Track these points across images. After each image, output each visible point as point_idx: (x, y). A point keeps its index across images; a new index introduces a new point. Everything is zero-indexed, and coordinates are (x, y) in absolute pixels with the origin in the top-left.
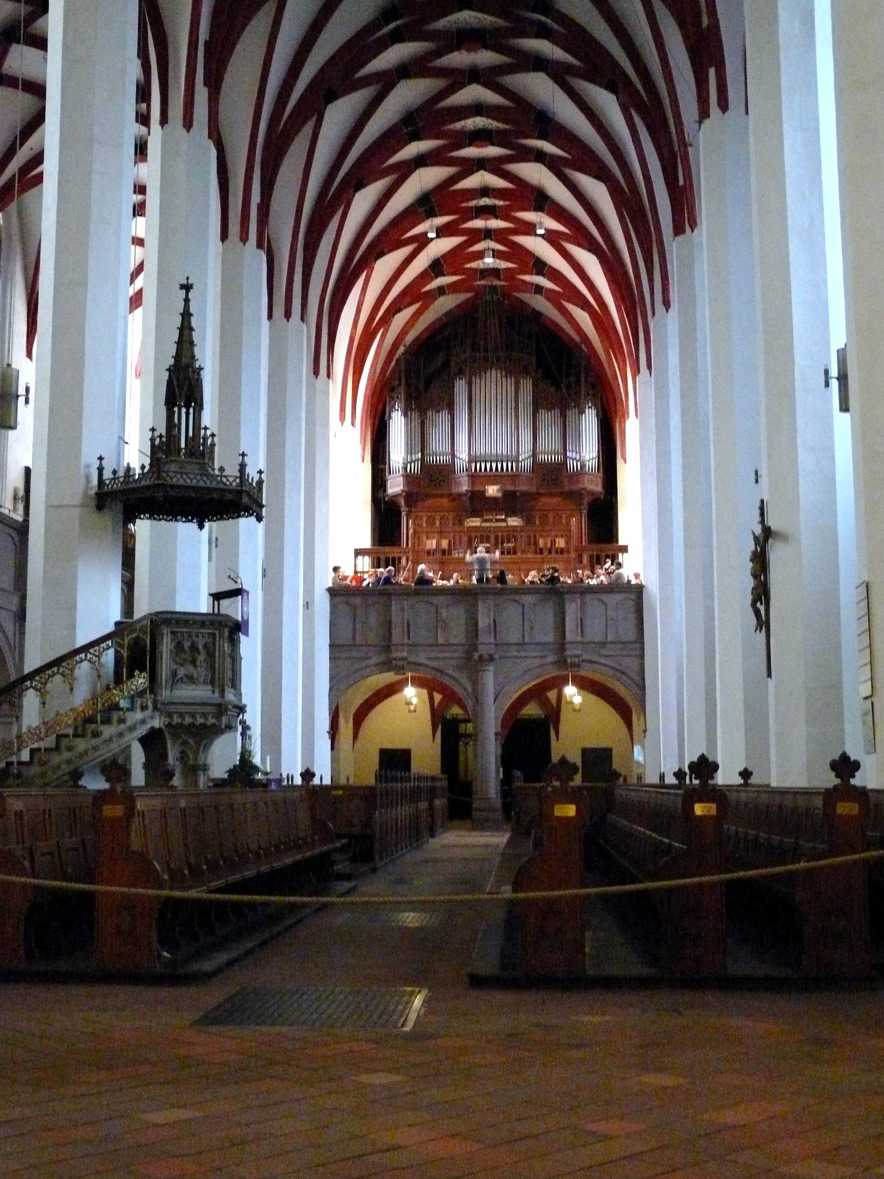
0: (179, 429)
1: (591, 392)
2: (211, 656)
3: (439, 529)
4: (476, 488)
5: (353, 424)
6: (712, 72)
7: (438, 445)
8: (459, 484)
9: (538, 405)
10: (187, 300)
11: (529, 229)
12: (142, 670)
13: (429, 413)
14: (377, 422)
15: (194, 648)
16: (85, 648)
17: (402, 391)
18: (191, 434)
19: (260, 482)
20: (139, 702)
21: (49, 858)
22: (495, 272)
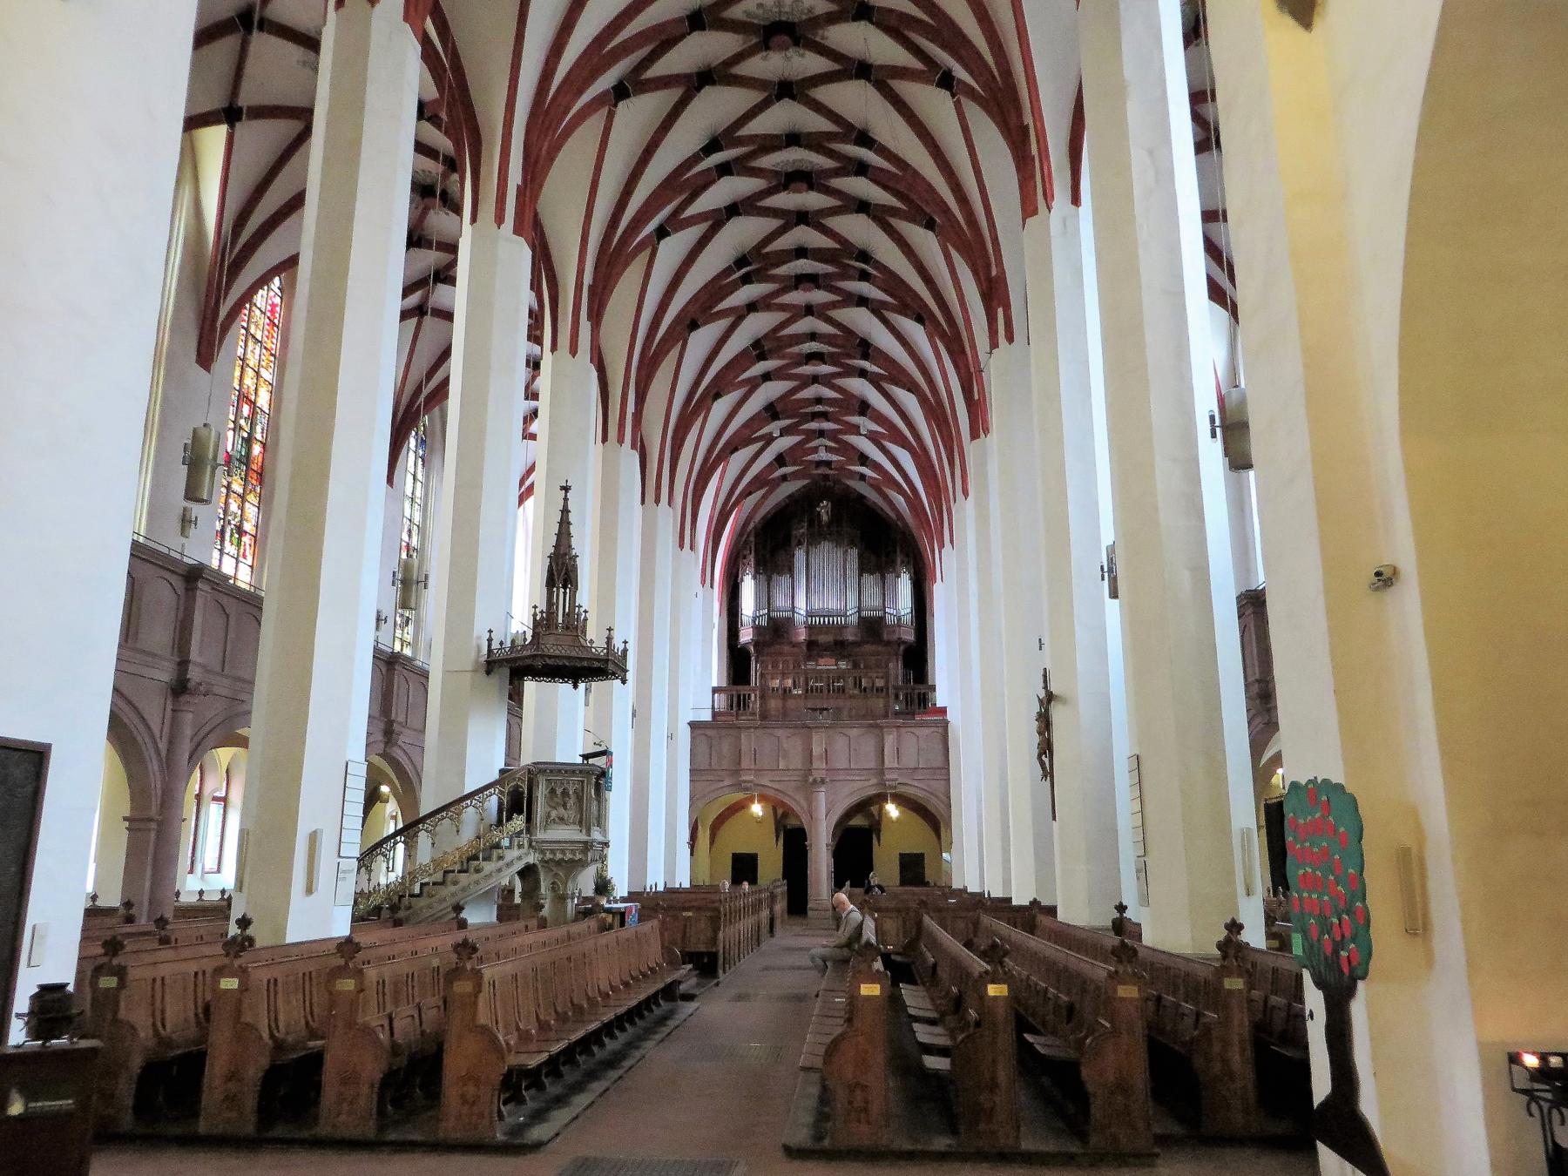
0: (557, 607)
1: (906, 559)
2: (580, 799)
4: (813, 638)
5: (712, 587)
6: (1000, 311)
7: (781, 601)
8: (797, 634)
9: (863, 569)
10: (566, 499)
11: (855, 430)
12: (520, 812)
13: (775, 577)
15: (565, 793)
16: (471, 795)
17: (752, 558)
18: (567, 610)
19: (625, 651)
20: (516, 840)
21: (410, 1019)
22: (828, 464)
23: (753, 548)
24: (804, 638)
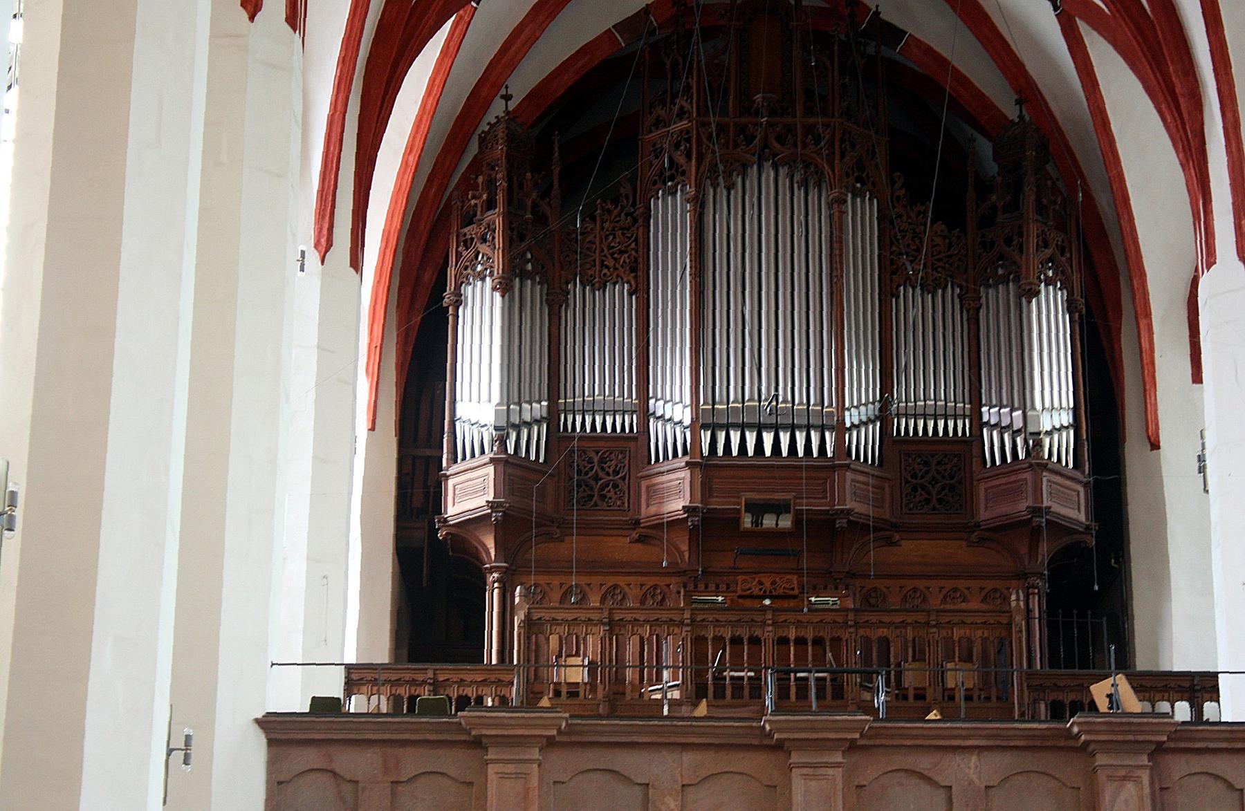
1: (1056, 237)
4: (717, 504)
5: (356, 262)
17: (496, 218)
23: (502, 183)
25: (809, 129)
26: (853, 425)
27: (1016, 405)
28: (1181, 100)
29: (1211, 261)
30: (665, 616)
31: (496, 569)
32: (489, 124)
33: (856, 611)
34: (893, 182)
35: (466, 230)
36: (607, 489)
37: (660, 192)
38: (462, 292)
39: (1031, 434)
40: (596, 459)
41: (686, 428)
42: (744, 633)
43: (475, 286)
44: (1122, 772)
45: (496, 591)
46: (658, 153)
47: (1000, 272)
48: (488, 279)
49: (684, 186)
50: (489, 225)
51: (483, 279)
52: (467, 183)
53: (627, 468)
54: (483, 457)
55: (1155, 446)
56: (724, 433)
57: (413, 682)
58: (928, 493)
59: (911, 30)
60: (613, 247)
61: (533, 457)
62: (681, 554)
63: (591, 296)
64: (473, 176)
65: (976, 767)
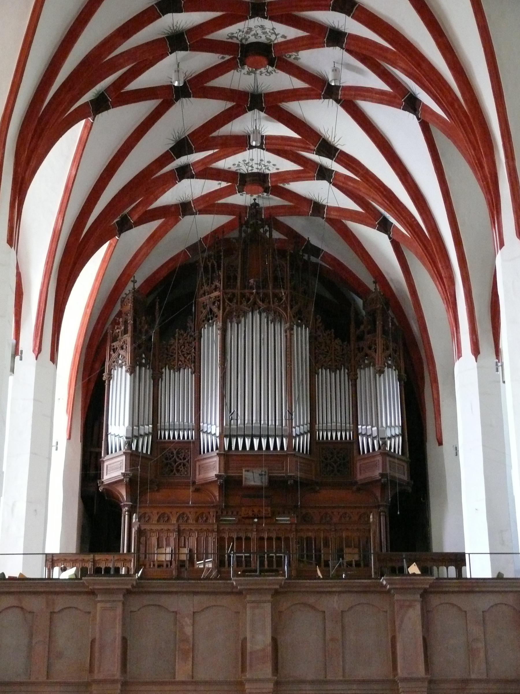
3: (176, 527)
4: (231, 473)
5: (53, 358)
8: (207, 469)
13: (166, 371)
14: (92, 386)
17: (128, 338)
23: (130, 322)
24: (217, 472)
25: (275, 295)
26: (297, 435)
27: (374, 425)
28: (445, 280)
29: (459, 355)
30: (205, 527)
31: (127, 505)
32: (126, 294)
33: (296, 524)
34: (316, 320)
35: (114, 344)
36: (180, 467)
37: (206, 325)
38: (112, 373)
39: (381, 439)
40: (175, 453)
41: (217, 437)
42: (243, 535)
43: (118, 370)
44: (407, 603)
45: (126, 516)
46: (205, 307)
47: (366, 362)
48: (124, 367)
49: (216, 323)
50: (124, 342)
51: (122, 367)
52: (115, 323)
53: (190, 456)
54: (121, 451)
55: (440, 443)
56: (235, 440)
57: (83, 561)
58: (333, 467)
59: (325, 249)
60: (184, 351)
61: (144, 452)
62: (215, 496)
63: (174, 375)
64: (118, 319)
65: (337, 602)
